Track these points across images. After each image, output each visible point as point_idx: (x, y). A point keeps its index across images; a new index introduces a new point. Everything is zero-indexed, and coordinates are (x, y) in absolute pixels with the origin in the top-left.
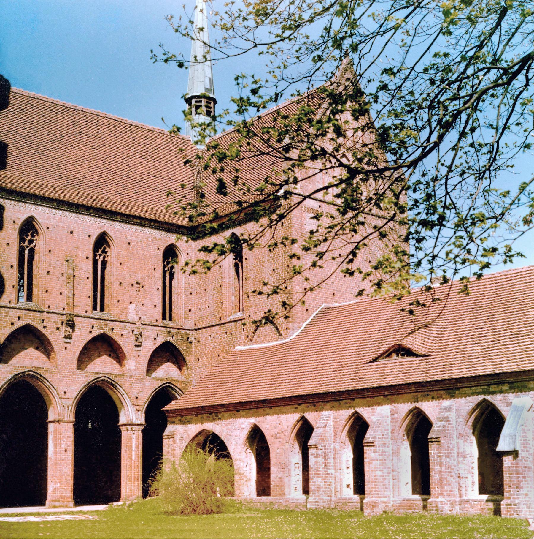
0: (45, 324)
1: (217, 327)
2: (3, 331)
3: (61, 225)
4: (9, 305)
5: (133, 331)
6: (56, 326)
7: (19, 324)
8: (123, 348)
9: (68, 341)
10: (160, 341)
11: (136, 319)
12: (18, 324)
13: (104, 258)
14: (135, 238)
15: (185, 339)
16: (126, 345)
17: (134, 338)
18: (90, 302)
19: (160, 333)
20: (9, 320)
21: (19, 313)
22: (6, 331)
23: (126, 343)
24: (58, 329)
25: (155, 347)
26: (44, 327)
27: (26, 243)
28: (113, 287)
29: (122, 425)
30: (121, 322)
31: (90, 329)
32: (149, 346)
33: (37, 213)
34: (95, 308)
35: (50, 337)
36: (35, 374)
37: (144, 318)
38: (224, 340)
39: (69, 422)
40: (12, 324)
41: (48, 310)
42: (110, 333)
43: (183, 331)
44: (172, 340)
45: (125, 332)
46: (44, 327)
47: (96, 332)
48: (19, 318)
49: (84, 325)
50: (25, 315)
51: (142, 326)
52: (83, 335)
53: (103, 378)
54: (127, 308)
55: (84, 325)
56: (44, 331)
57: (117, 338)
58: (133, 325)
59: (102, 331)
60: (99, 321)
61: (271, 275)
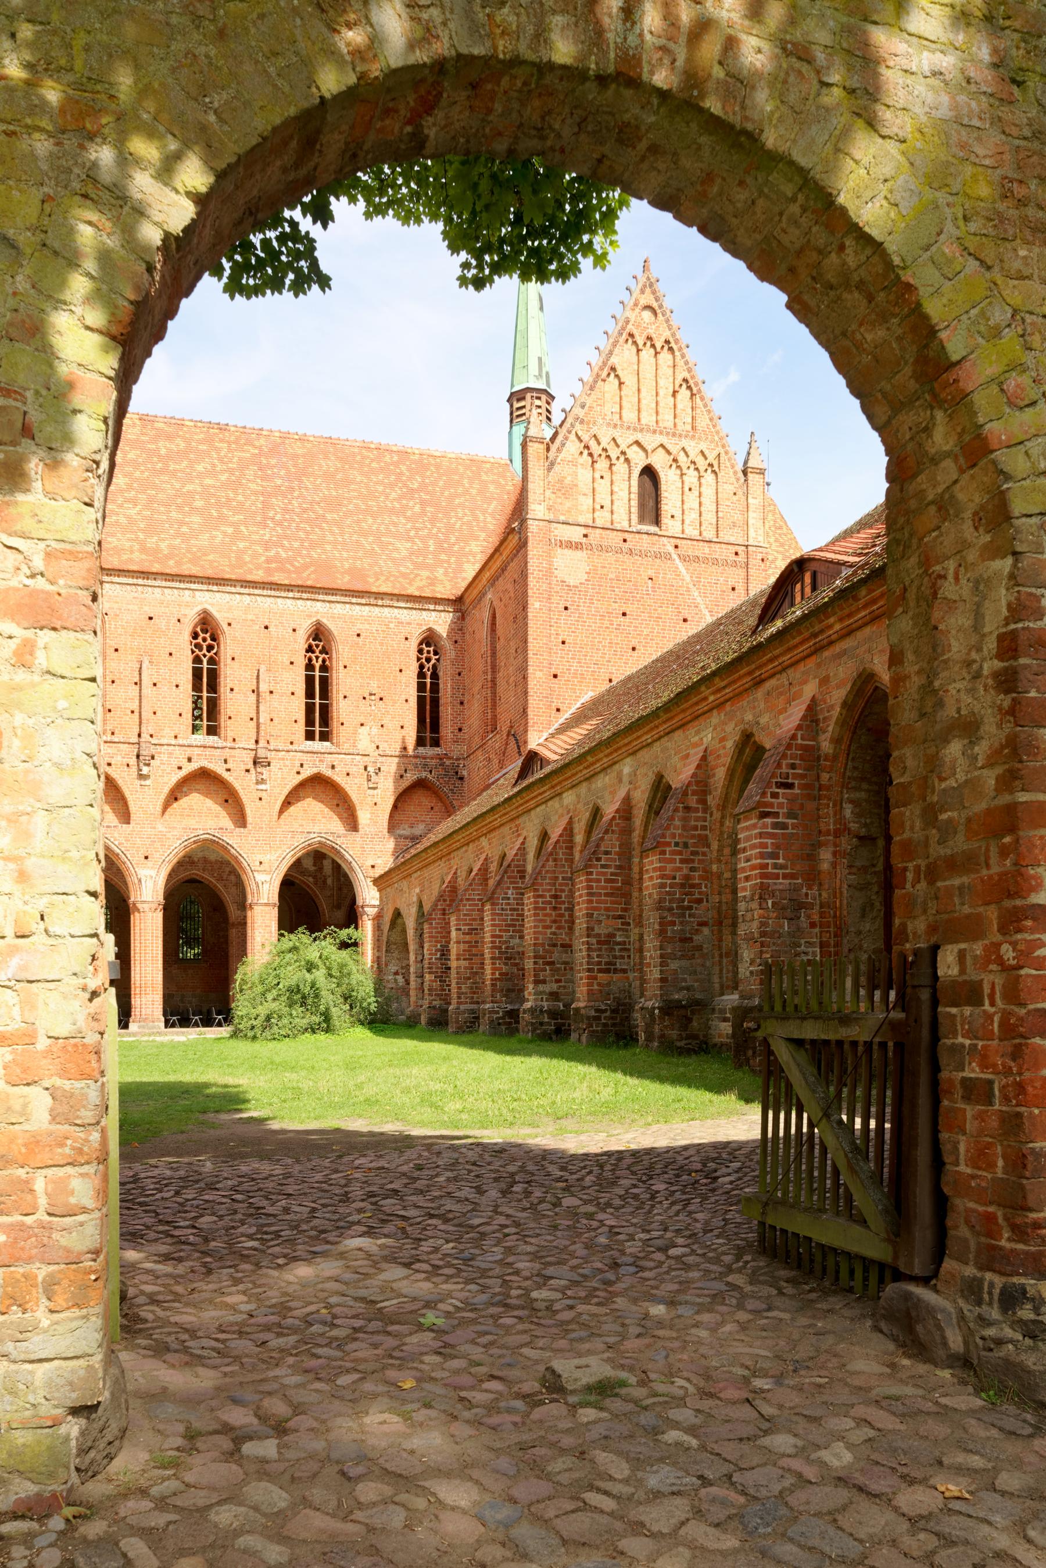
0: (228, 766)
2: (166, 779)
3: (250, 617)
4: (173, 742)
5: (366, 768)
6: (244, 767)
12: (189, 768)
13: (324, 661)
14: (367, 626)
15: (452, 773)
16: (355, 787)
18: (301, 727)
19: (410, 767)
20: (175, 763)
21: (189, 752)
23: (354, 787)
24: (248, 771)
26: (228, 770)
27: (205, 651)
31: (297, 768)
33: (212, 605)
34: (310, 736)
35: (237, 785)
39: (266, 905)
40: (180, 768)
41: (233, 745)
42: (328, 773)
43: (448, 762)
45: (353, 770)
46: (228, 770)
47: (307, 772)
48: (189, 760)
49: (288, 763)
51: (381, 759)
52: (283, 777)
54: (355, 733)
55: (288, 763)
56: (226, 775)
57: (339, 778)
58: (366, 759)
59: (315, 770)
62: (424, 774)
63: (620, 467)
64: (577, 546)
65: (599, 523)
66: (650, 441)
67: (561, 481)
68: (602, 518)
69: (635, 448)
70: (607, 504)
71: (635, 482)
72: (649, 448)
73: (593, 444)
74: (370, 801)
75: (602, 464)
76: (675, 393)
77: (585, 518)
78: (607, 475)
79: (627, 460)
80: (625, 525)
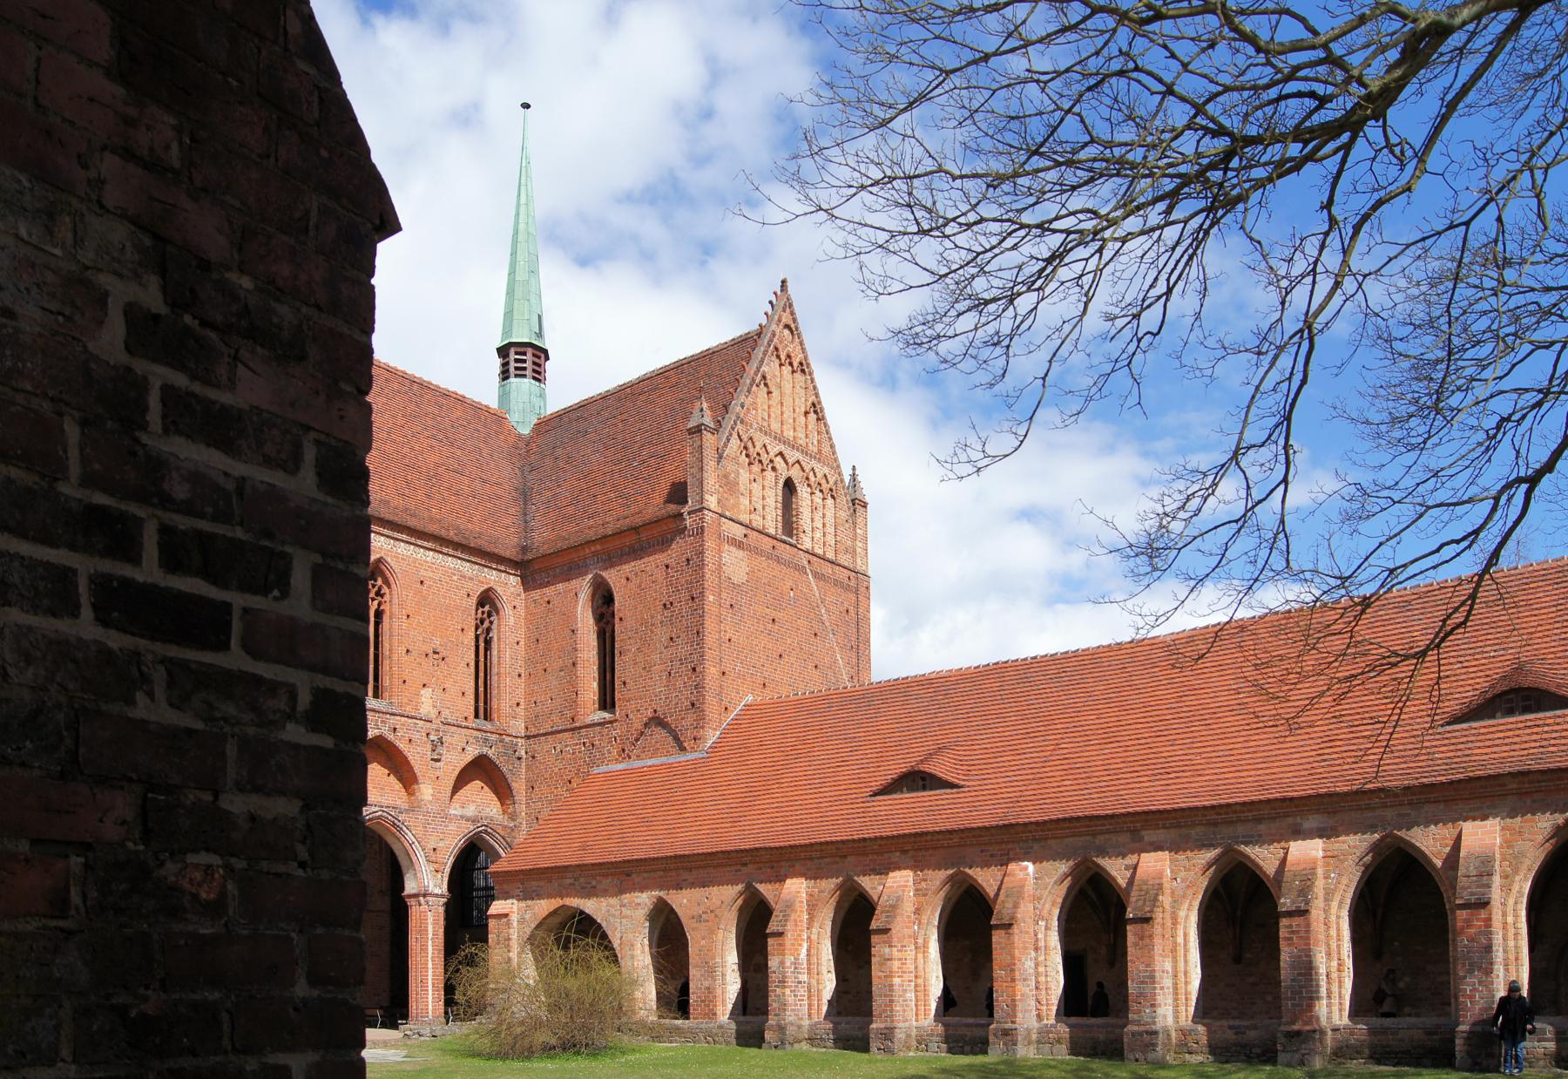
1: (566, 734)
8: (412, 762)
10: (472, 752)
11: (433, 715)
17: (429, 746)
23: (417, 755)
25: (463, 764)
28: (395, 657)
29: (410, 896)
32: (454, 761)
37: (446, 713)
44: (491, 753)
45: (416, 736)
51: (443, 727)
62: (485, 750)
63: (769, 474)
64: (739, 545)
65: (754, 525)
66: (793, 456)
67: (726, 476)
68: (757, 522)
69: (779, 459)
70: (759, 507)
71: (780, 493)
72: (790, 461)
73: (750, 445)
74: (432, 774)
75: (756, 468)
76: (806, 413)
77: (744, 518)
78: (759, 480)
79: (774, 469)
80: (772, 531)
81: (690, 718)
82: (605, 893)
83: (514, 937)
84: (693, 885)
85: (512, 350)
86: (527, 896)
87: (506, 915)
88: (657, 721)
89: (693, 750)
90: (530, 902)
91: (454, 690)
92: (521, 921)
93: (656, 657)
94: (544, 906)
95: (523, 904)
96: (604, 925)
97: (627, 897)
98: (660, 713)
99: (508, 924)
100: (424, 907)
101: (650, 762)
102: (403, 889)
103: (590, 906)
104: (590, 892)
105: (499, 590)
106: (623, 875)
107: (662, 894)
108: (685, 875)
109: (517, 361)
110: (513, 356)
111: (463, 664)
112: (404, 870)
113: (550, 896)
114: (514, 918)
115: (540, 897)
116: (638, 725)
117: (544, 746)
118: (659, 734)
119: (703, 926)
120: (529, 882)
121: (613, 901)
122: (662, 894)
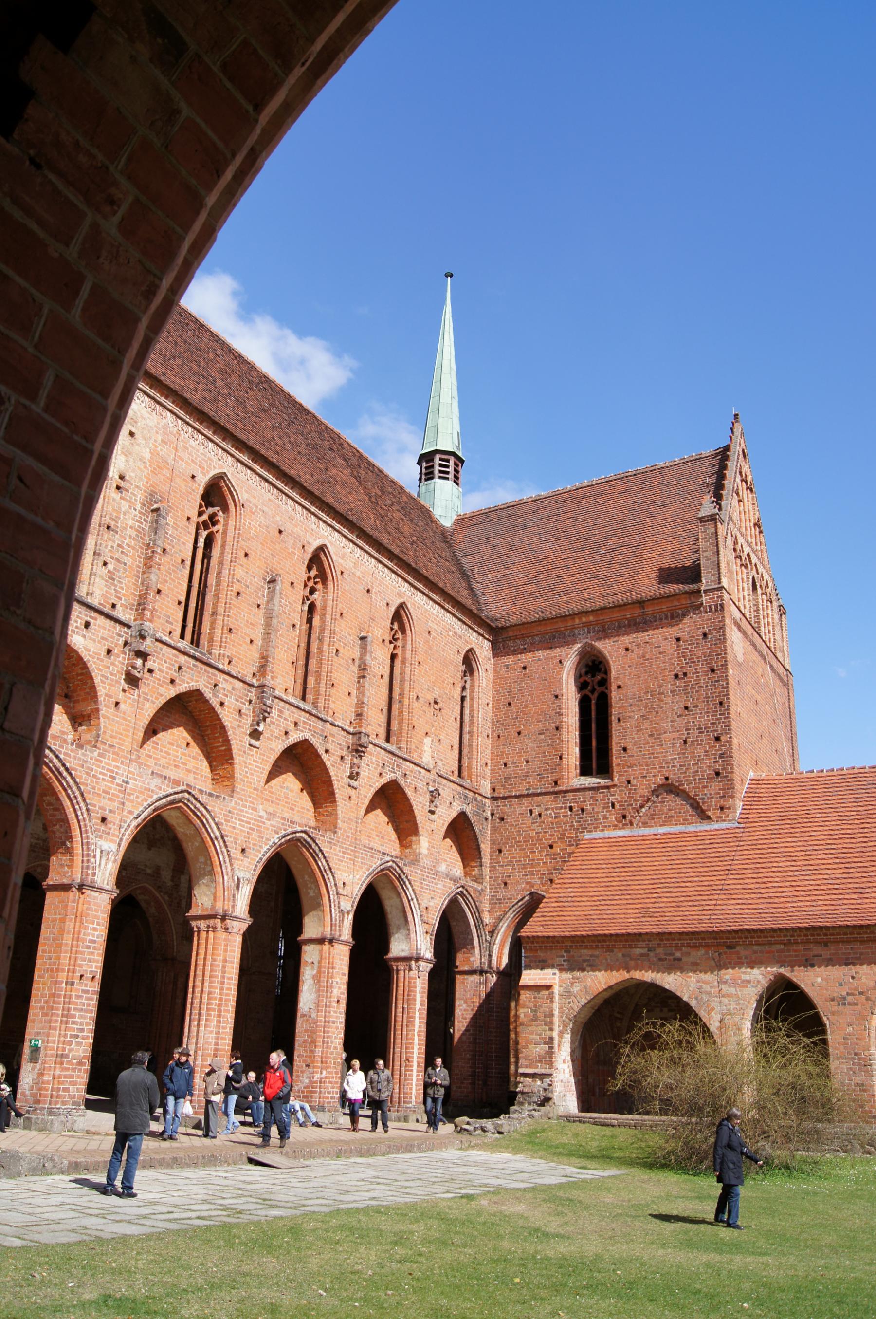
1: (547, 798)
2: (273, 746)
7: (295, 736)
9: (355, 784)
20: (283, 725)
22: (277, 747)
30: (415, 764)
31: (379, 770)
36: (309, 840)
37: (440, 764)
38: (565, 819)
50: (305, 723)
53: (390, 864)
56: (325, 757)
60: (390, 756)
61: (680, 716)
81: (715, 786)
82: (695, 967)
83: (556, 1013)
84: (830, 962)
85: (437, 457)
86: (574, 965)
87: (548, 987)
88: (669, 788)
89: (719, 819)
90: (578, 974)
91: (446, 743)
92: (567, 994)
93: (666, 725)
94: (600, 980)
95: (568, 976)
96: (693, 1004)
97: (728, 974)
98: (673, 779)
99: (551, 998)
100: (414, 973)
101: (662, 830)
102: (387, 950)
103: (670, 981)
104: (673, 965)
105: (477, 651)
106: (725, 947)
107: (782, 970)
108: (817, 950)
109: (441, 465)
110: (437, 461)
111: (453, 719)
112: (392, 929)
113: (609, 968)
114: (556, 990)
115: (594, 967)
116: (642, 789)
117: (515, 810)
118: (673, 802)
119: (848, 1009)
120: (575, 951)
121: (708, 977)
122: (782, 970)
